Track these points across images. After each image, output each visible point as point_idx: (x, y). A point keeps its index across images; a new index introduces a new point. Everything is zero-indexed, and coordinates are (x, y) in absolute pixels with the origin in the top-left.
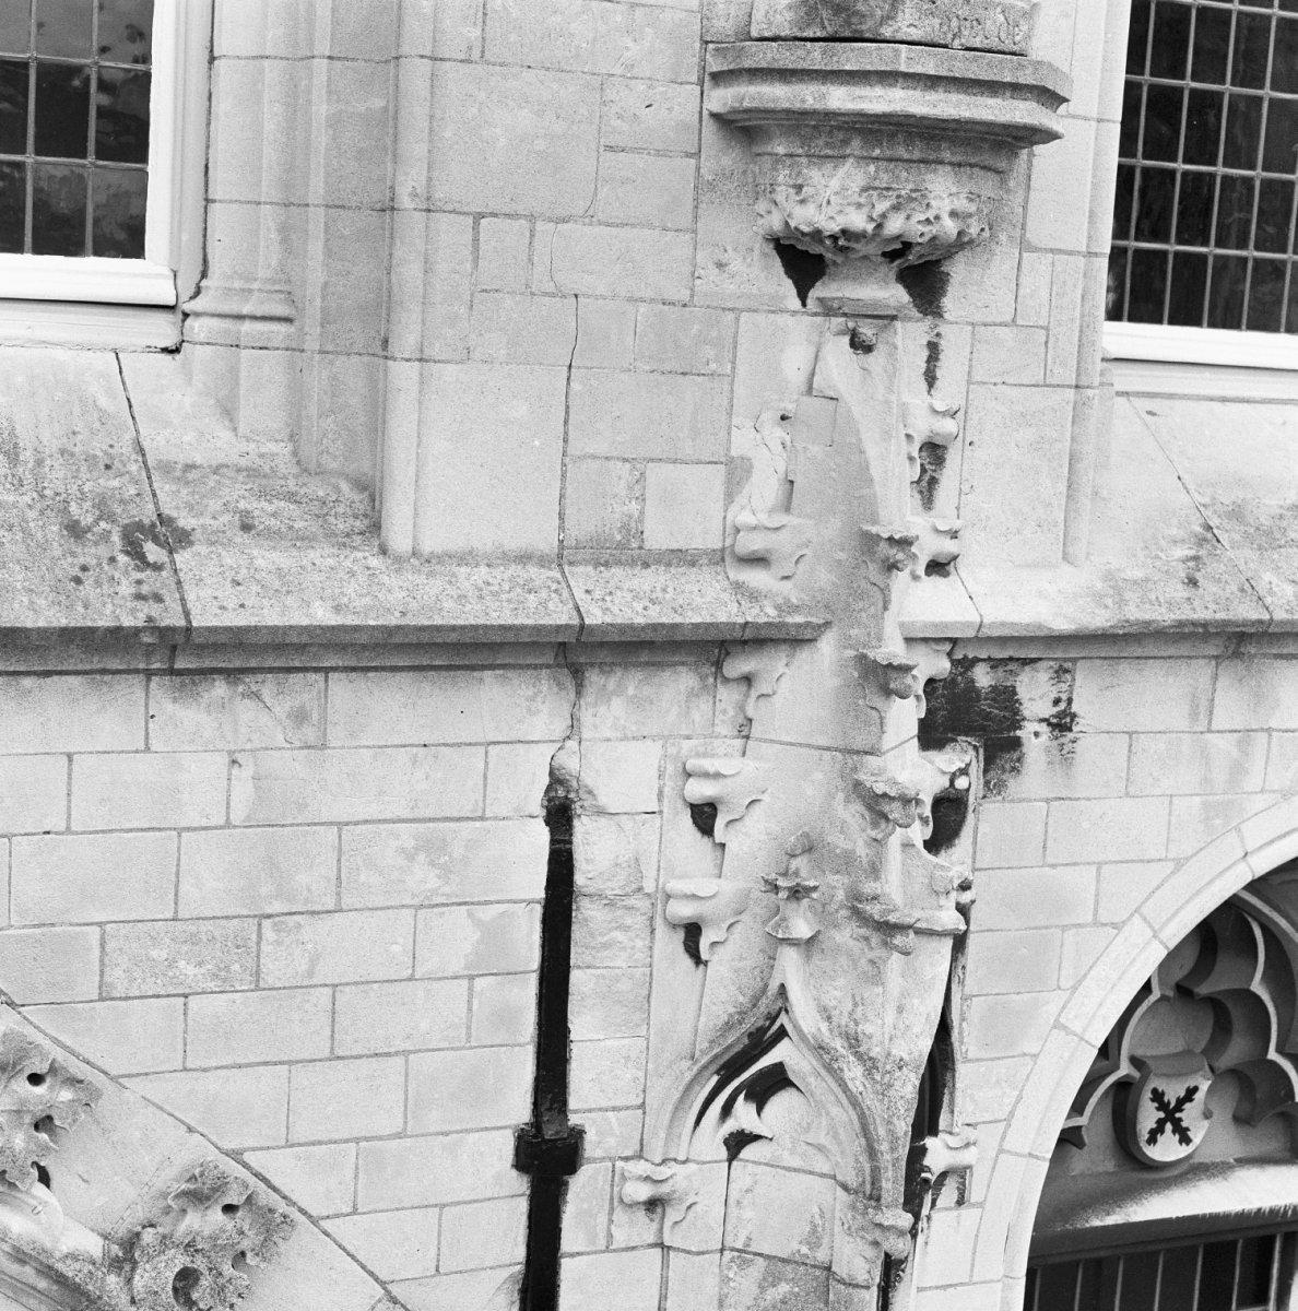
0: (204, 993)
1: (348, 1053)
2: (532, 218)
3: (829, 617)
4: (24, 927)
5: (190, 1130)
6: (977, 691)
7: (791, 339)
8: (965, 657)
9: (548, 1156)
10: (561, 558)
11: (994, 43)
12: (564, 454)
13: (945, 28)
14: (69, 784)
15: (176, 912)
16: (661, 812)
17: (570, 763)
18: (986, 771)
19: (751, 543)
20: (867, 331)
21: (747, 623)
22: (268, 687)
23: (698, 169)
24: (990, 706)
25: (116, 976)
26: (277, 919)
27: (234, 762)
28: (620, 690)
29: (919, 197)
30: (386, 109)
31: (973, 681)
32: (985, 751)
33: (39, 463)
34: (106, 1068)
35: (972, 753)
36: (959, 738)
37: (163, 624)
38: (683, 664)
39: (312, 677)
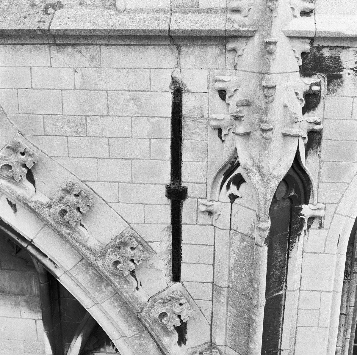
0: (72, 136)
1: (114, 157)
3: (257, 29)
4: (23, 114)
5: (71, 174)
6: (324, 58)
8: (319, 46)
9: (177, 195)
10: (172, 11)
14: (31, 75)
15: (63, 113)
16: (208, 92)
17: (178, 76)
18: (328, 86)
21: (226, 30)
22: (83, 49)
24: (329, 63)
25: (48, 129)
26: (91, 117)
27: (75, 71)
28: (192, 53)
31: (322, 54)
32: (327, 78)
34: (47, 154)
35: (322, 79)
36: (317, 74)
37: (42, 28)
38: (214, 45)
39: (95, 46)
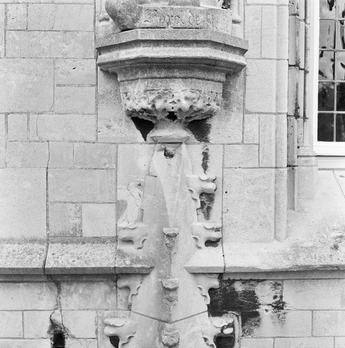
2: (28, 113)
3: (153, 265)
6: (237, 293)
7: (141, 153)
8: (229, 279)
10: (48, 241)
11: (187, 25)
12: (47, 201)
13: (162, 21)
16: (97, 338)
17: (58, 319)
18: (243, 325)
19: (123, 234)
20: (170, 149)
21: (115, 268)
23: (97, 90)
24: (243, 299)
28: (76, 291)
29: (167, 92)
31: (234, 289)
32: (242, 317)
35: (236, 318)
36: (229, 312)
38: (102, 281)
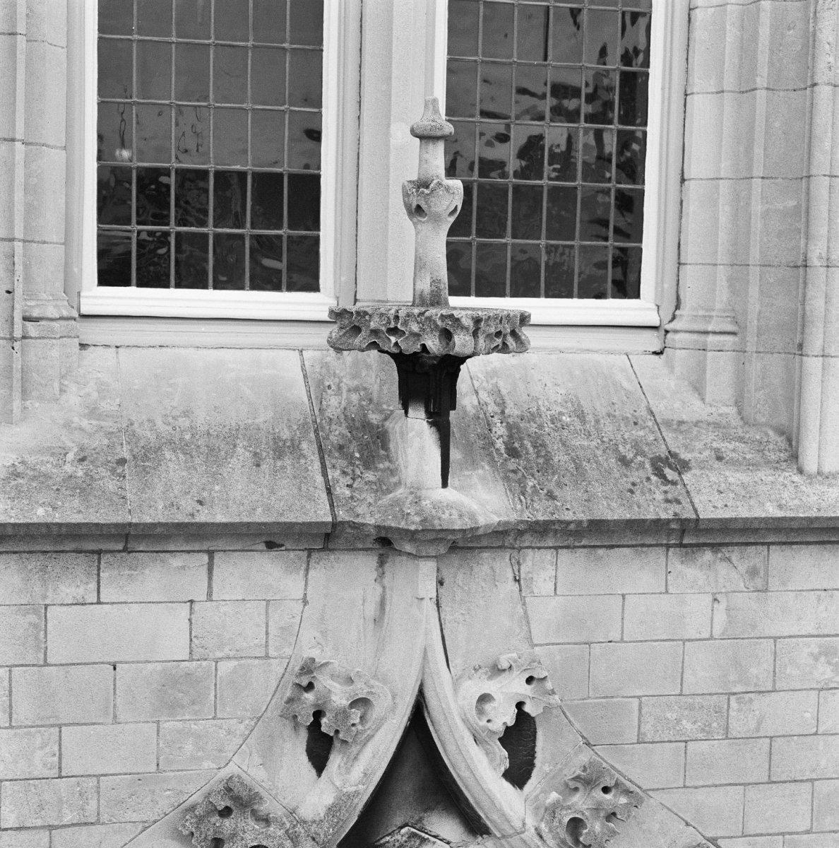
0: (696, 740)
1: (779, 780)
4: (597, 698)
5: (687, 824)
14: (623, 612)
15: (681, 690)
22: (735, 554)
25: (647, 728)
26: (739, 696)
27: (715, 600)
30: (798, 207)
33: (597, 421)
34: (640, 784)
37: (683, 517)
39: (760, 548)
